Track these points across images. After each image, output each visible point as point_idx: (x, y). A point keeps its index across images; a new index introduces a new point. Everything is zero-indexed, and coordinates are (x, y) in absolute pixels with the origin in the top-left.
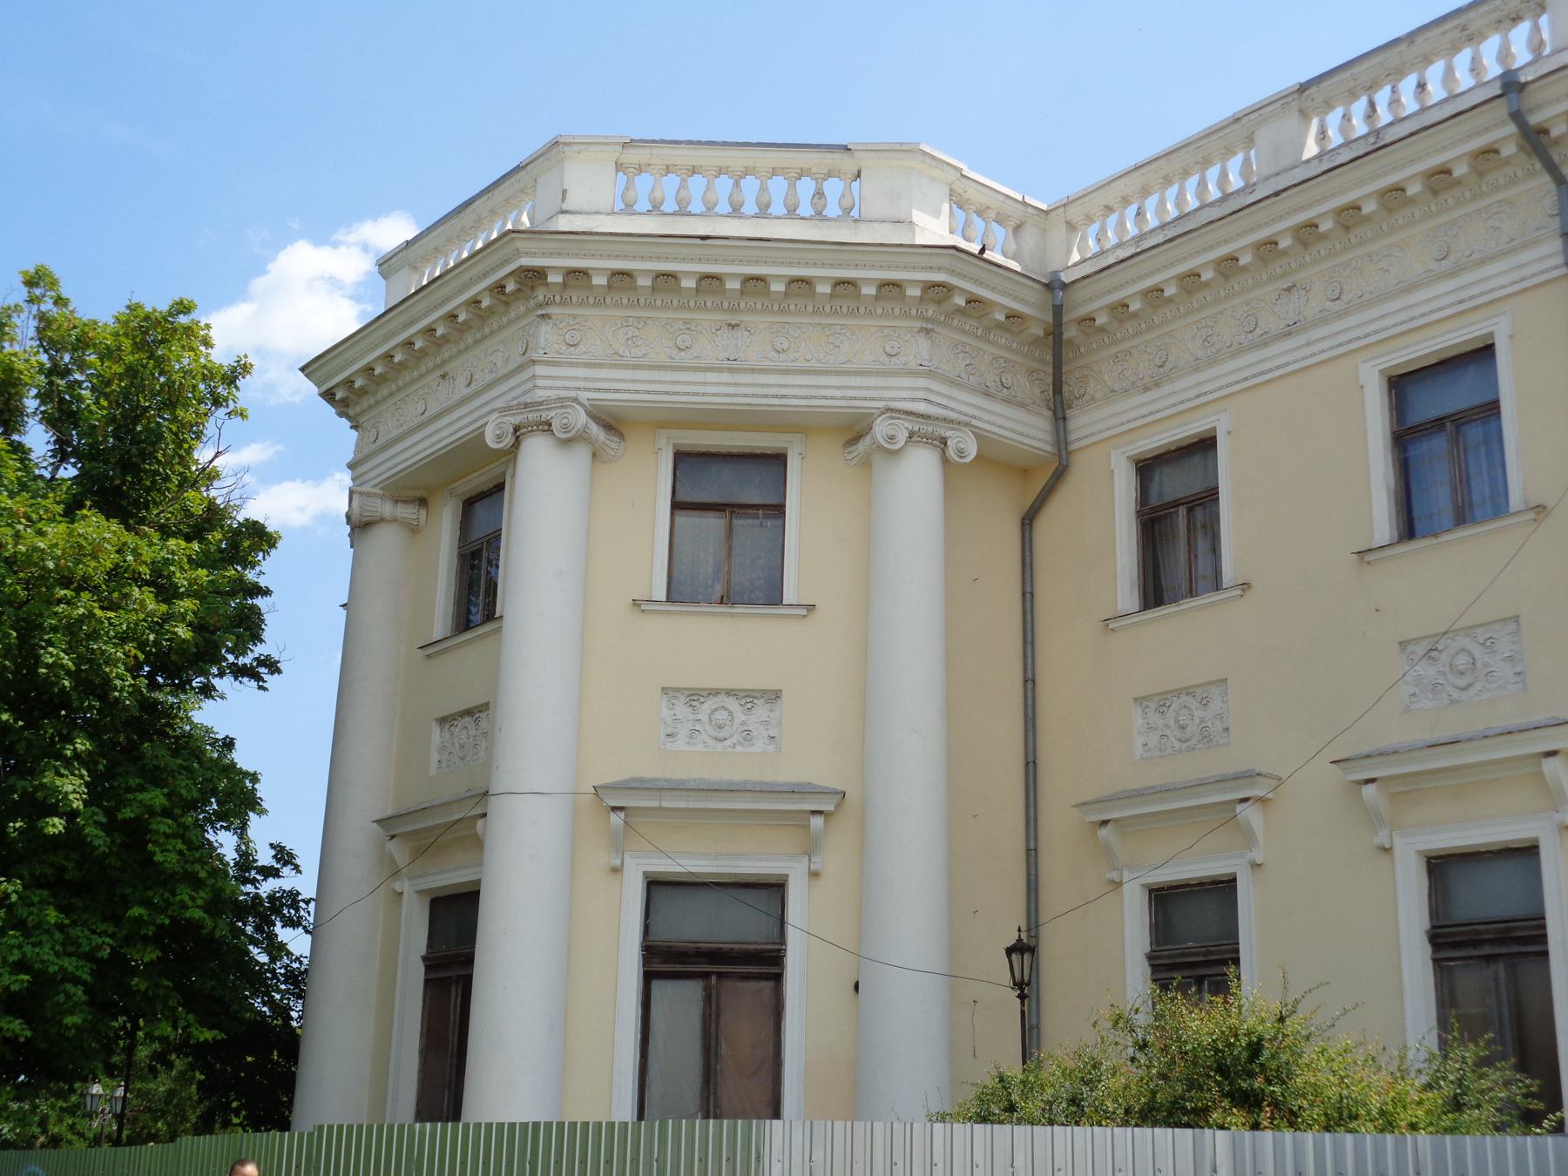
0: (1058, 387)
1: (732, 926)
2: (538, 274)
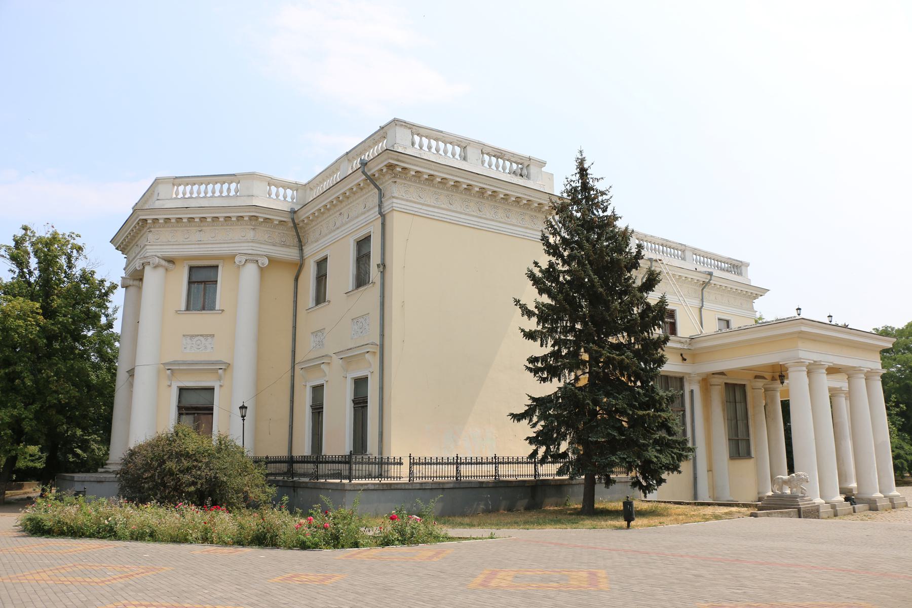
0: (300, 241)
2: (146, 220)
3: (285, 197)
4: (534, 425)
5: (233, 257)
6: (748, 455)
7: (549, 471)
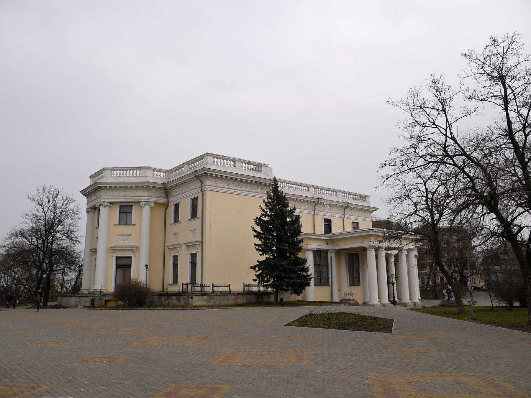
0: (167, 195)
1: (125, 262)
3: (160, 176)
4: (256, 272)
5: (139, 202)
6: (359, 284)
7: (263, 289)
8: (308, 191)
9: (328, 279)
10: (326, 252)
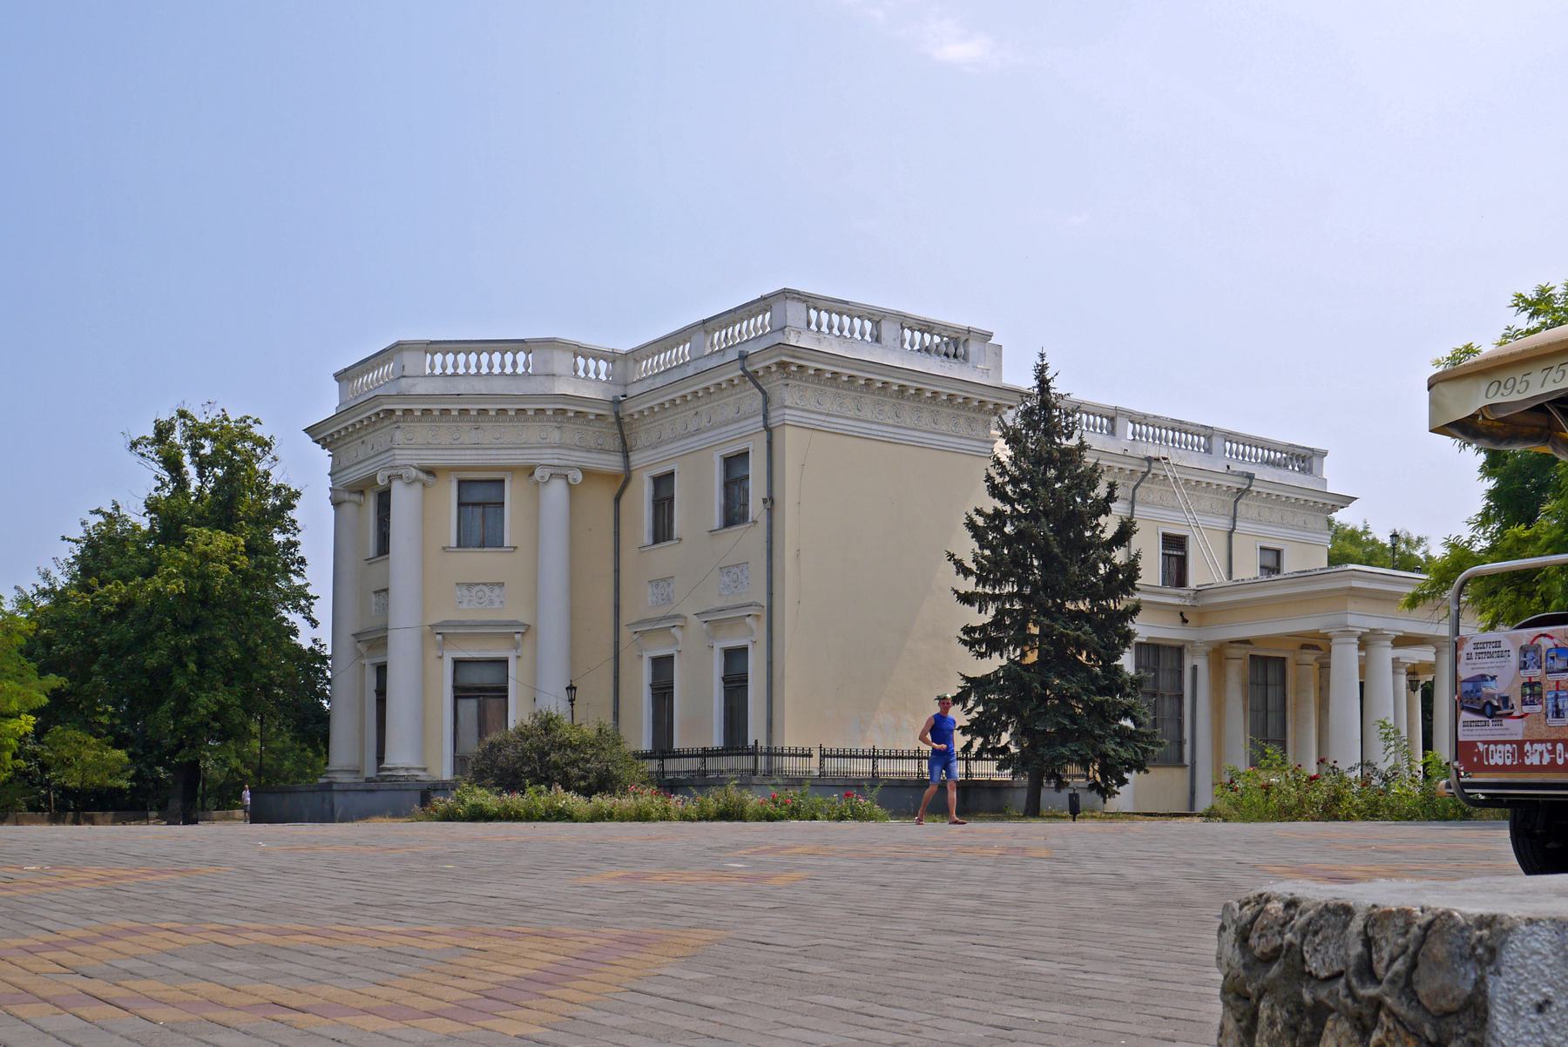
1: (486, 677)
3: (597, 373)
4: (969, 711)
5: (530, 470)
8: (1112, 432)
9: (1180, 743)
10: (1178, 651)
